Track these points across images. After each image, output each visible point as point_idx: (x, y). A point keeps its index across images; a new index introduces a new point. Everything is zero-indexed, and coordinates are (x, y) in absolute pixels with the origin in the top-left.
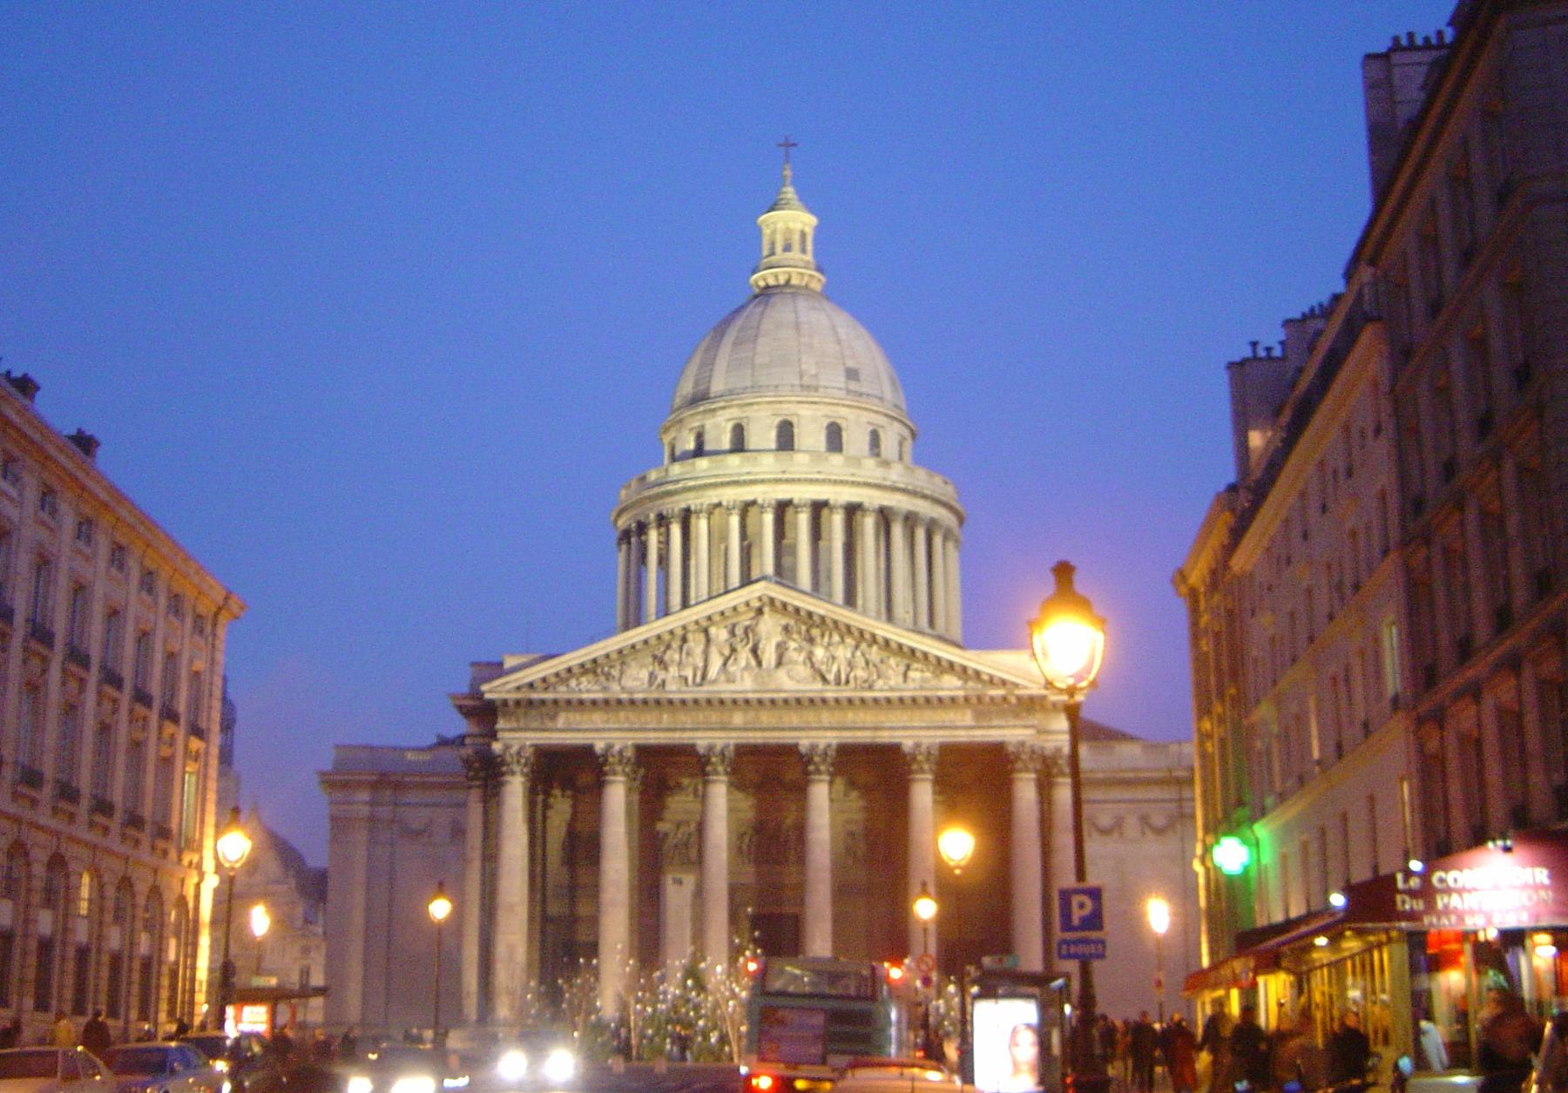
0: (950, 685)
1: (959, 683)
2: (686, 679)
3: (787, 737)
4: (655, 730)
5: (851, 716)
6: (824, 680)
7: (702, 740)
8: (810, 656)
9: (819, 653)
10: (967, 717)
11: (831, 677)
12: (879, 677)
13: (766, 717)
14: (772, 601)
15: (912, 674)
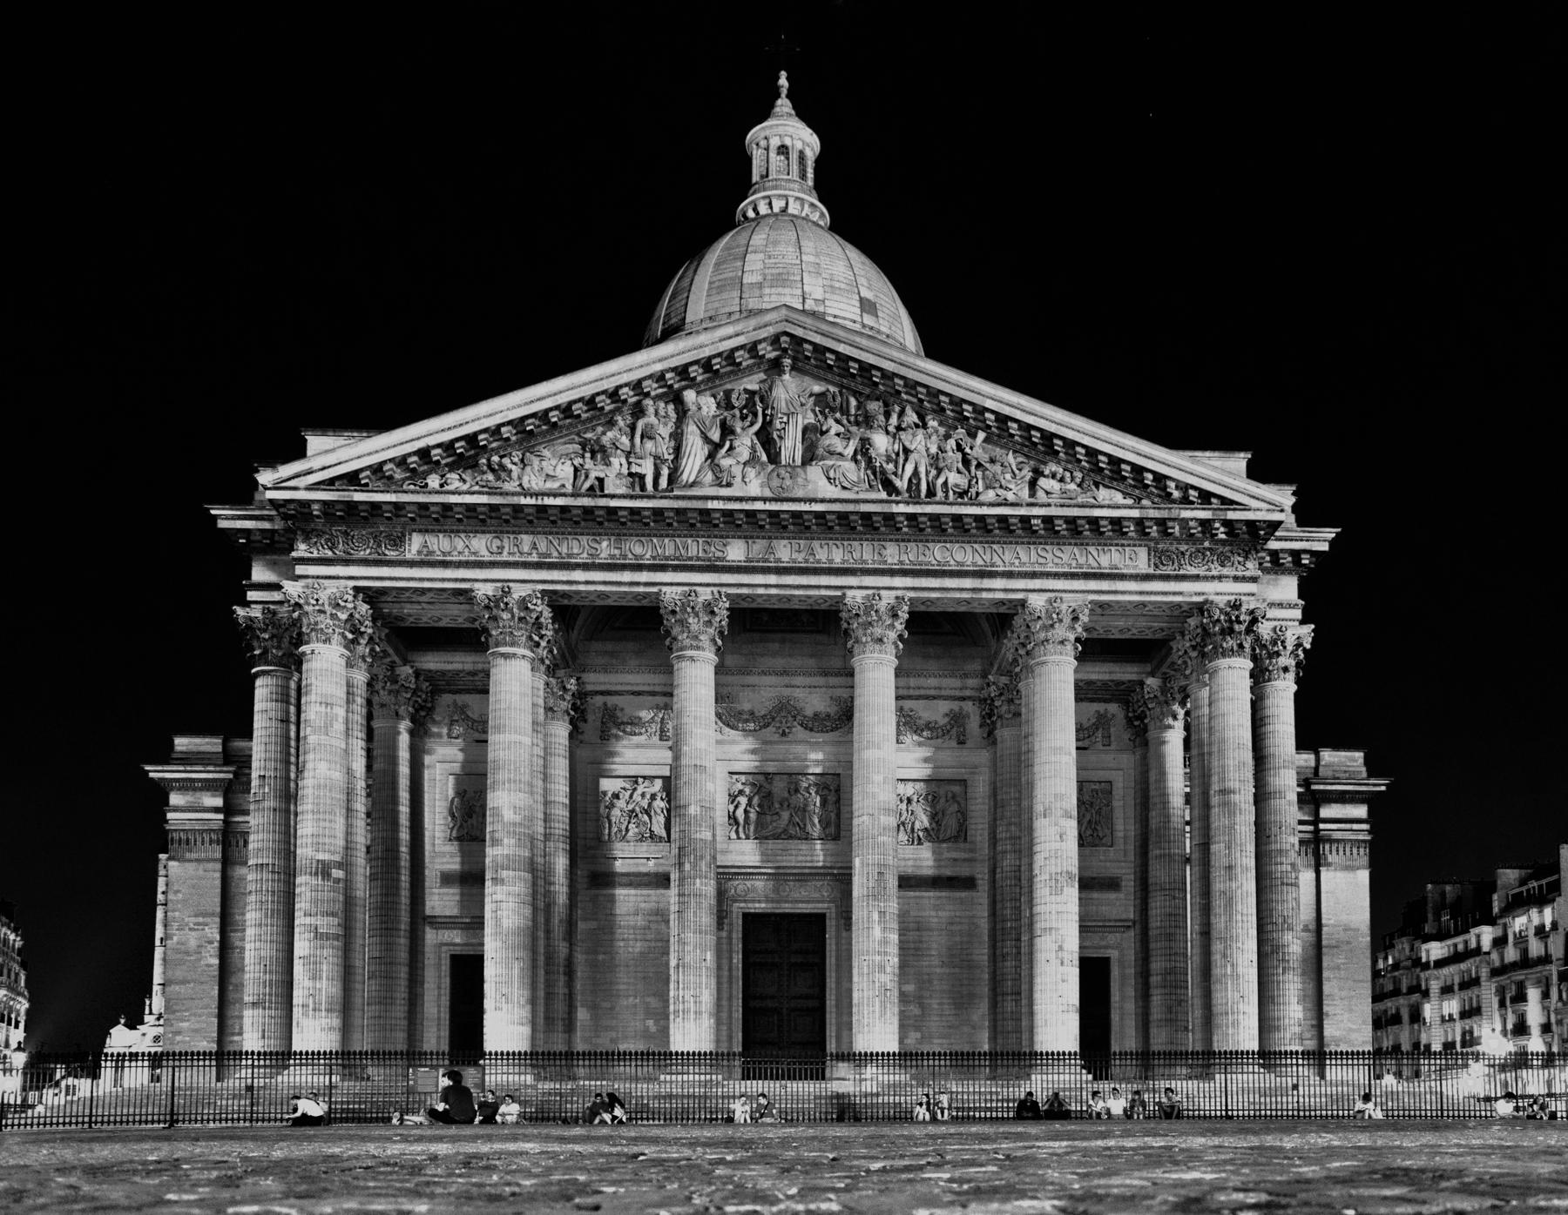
0: (1111, 502)
1: (1130, 502)
2: (642, 477)
3: (821, 586)
4: (585, 567)
5: (938, 554)
6: (889, 486)
7: (671, 587)
8: (865, 443)
9: (881, 443)
10: (1141, 560)
11: (902, 484)
12: (987, 487)
13: (785, 552)
14: (798, 341)
15: (1042, 482)
